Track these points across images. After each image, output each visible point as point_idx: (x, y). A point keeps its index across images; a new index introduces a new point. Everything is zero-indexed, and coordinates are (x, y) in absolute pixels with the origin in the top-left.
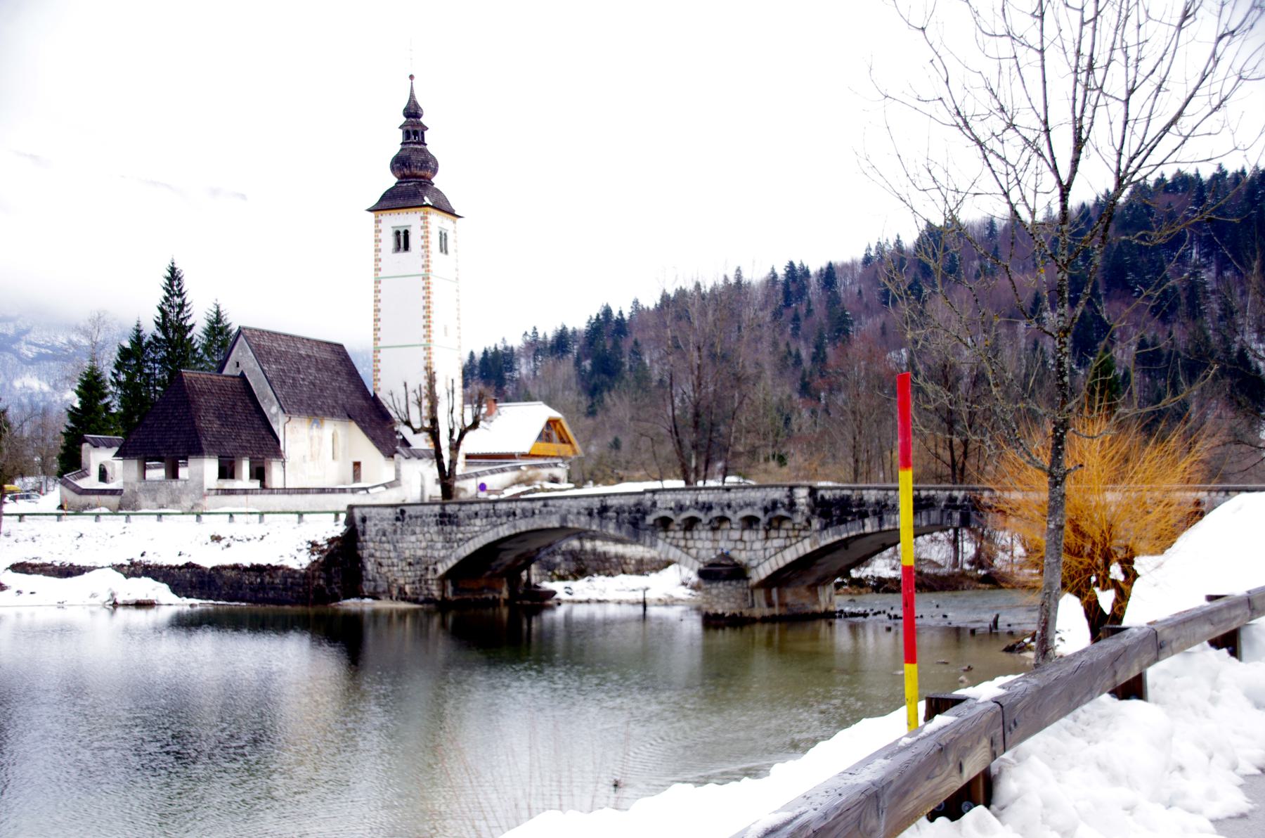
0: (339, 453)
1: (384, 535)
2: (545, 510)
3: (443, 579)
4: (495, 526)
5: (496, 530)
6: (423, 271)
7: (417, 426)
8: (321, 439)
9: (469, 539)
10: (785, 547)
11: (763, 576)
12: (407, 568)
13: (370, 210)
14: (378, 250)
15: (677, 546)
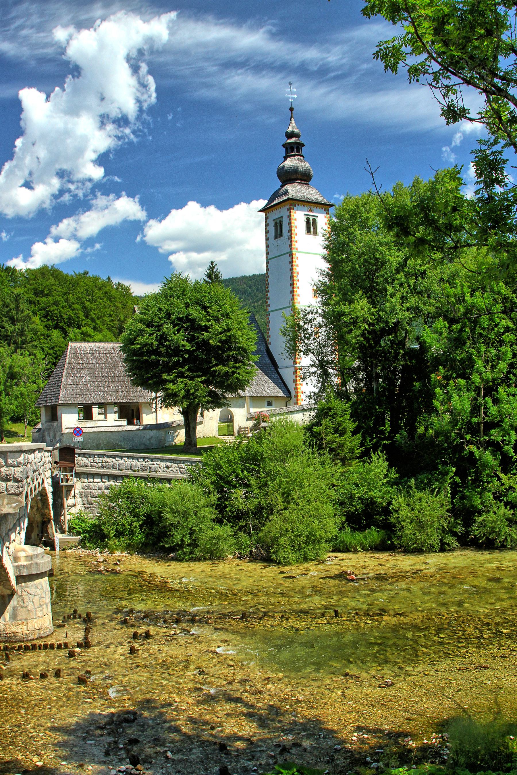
13: (261, 211)
14: (267, 239)
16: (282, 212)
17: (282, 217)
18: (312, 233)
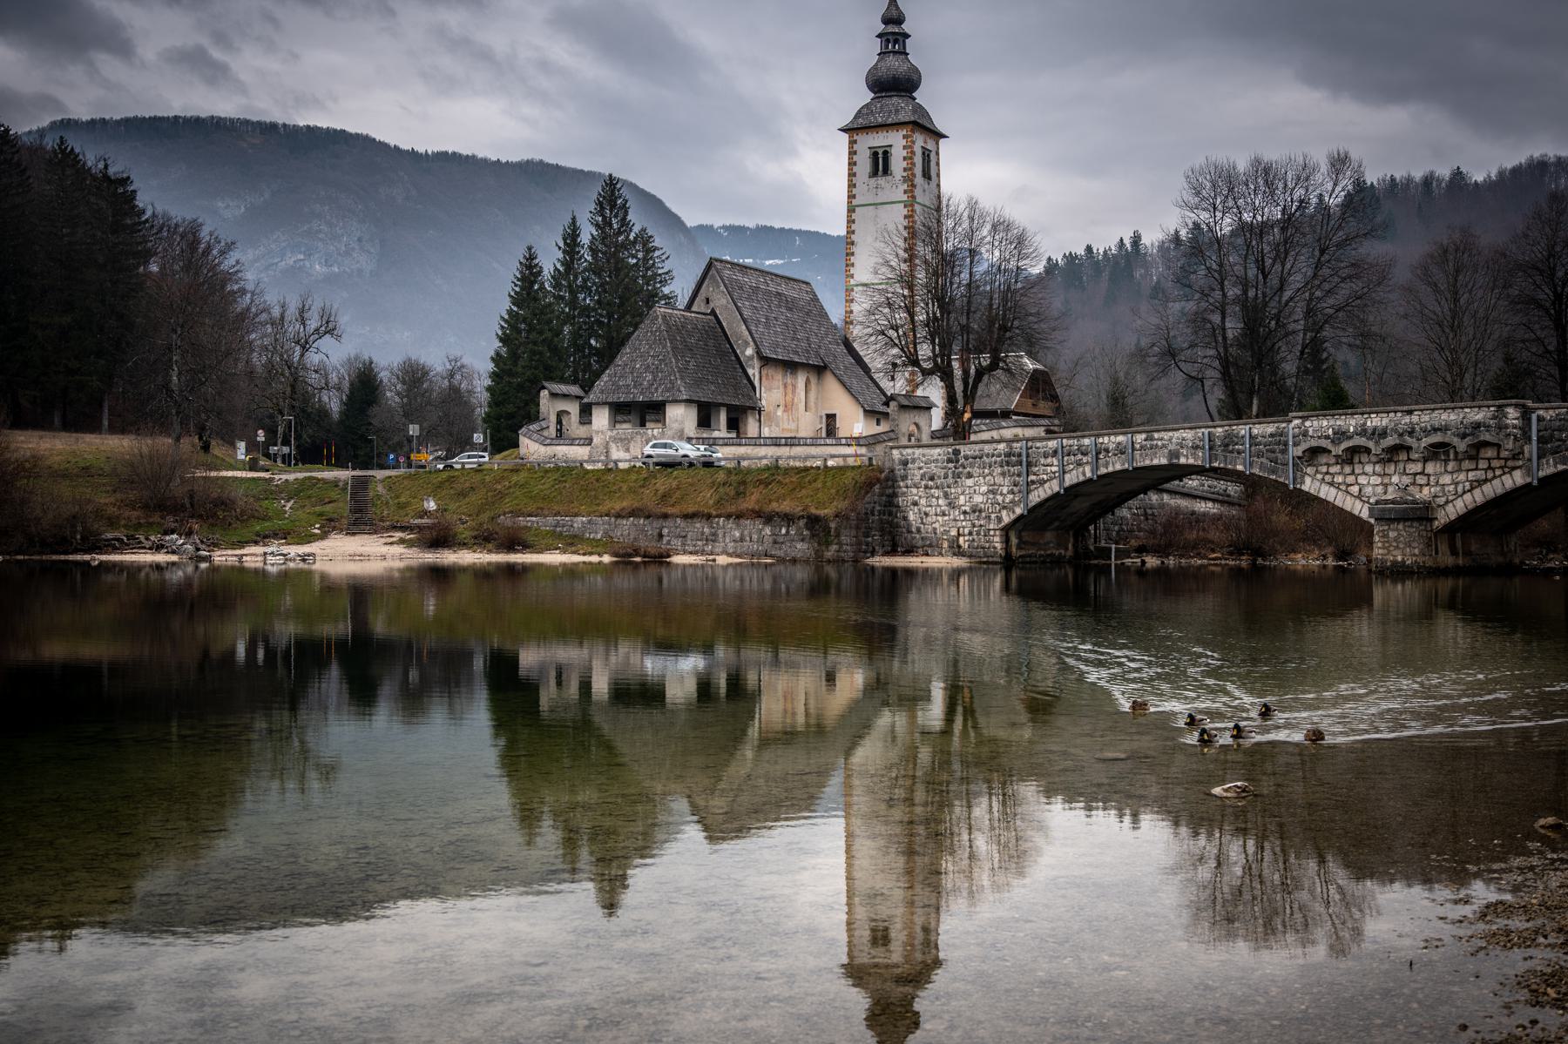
0: (812, 403)
1: (932, 479)
2: (1148, 443)
3: (1006, 530)
4: (1079, 464)
5: (1081, 469)
6: (905, 198)
7: (927, 365)
8: (794, 387)
9: (1045, 482)
10: (1486, 481)
11: (1453, 517)
12: (962, 517)
14: (852, 175)
15: (1331, 484)
16: (895, 141)
17: (891, 146)
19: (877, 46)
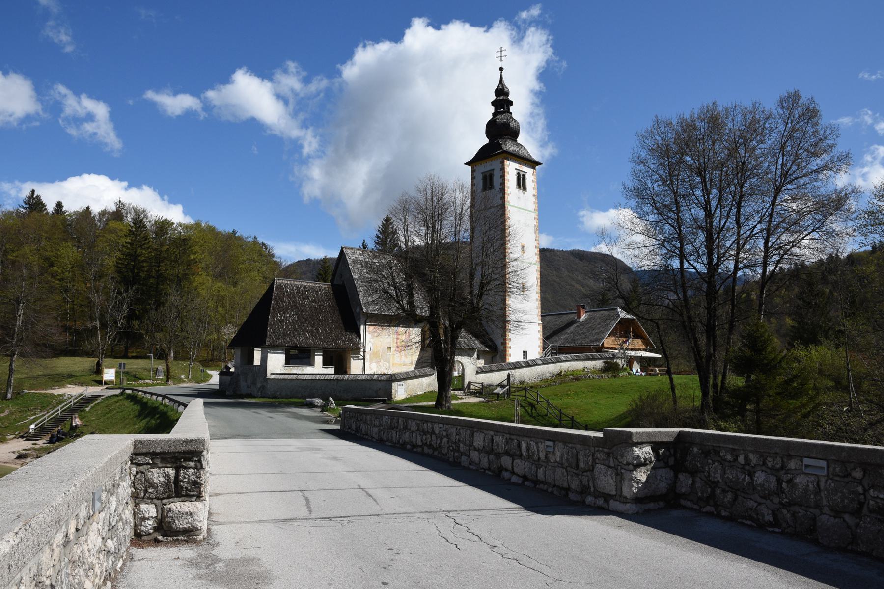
6: (501, 202)
13: (468, 164)
17: (493, 170)
18: (522, 188)
19: (492, 109)
